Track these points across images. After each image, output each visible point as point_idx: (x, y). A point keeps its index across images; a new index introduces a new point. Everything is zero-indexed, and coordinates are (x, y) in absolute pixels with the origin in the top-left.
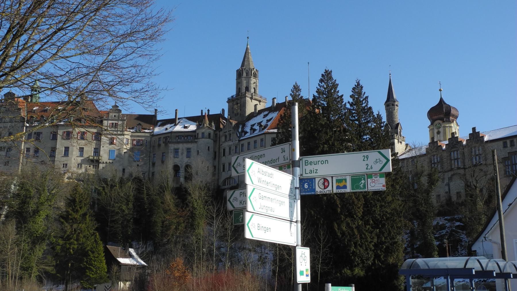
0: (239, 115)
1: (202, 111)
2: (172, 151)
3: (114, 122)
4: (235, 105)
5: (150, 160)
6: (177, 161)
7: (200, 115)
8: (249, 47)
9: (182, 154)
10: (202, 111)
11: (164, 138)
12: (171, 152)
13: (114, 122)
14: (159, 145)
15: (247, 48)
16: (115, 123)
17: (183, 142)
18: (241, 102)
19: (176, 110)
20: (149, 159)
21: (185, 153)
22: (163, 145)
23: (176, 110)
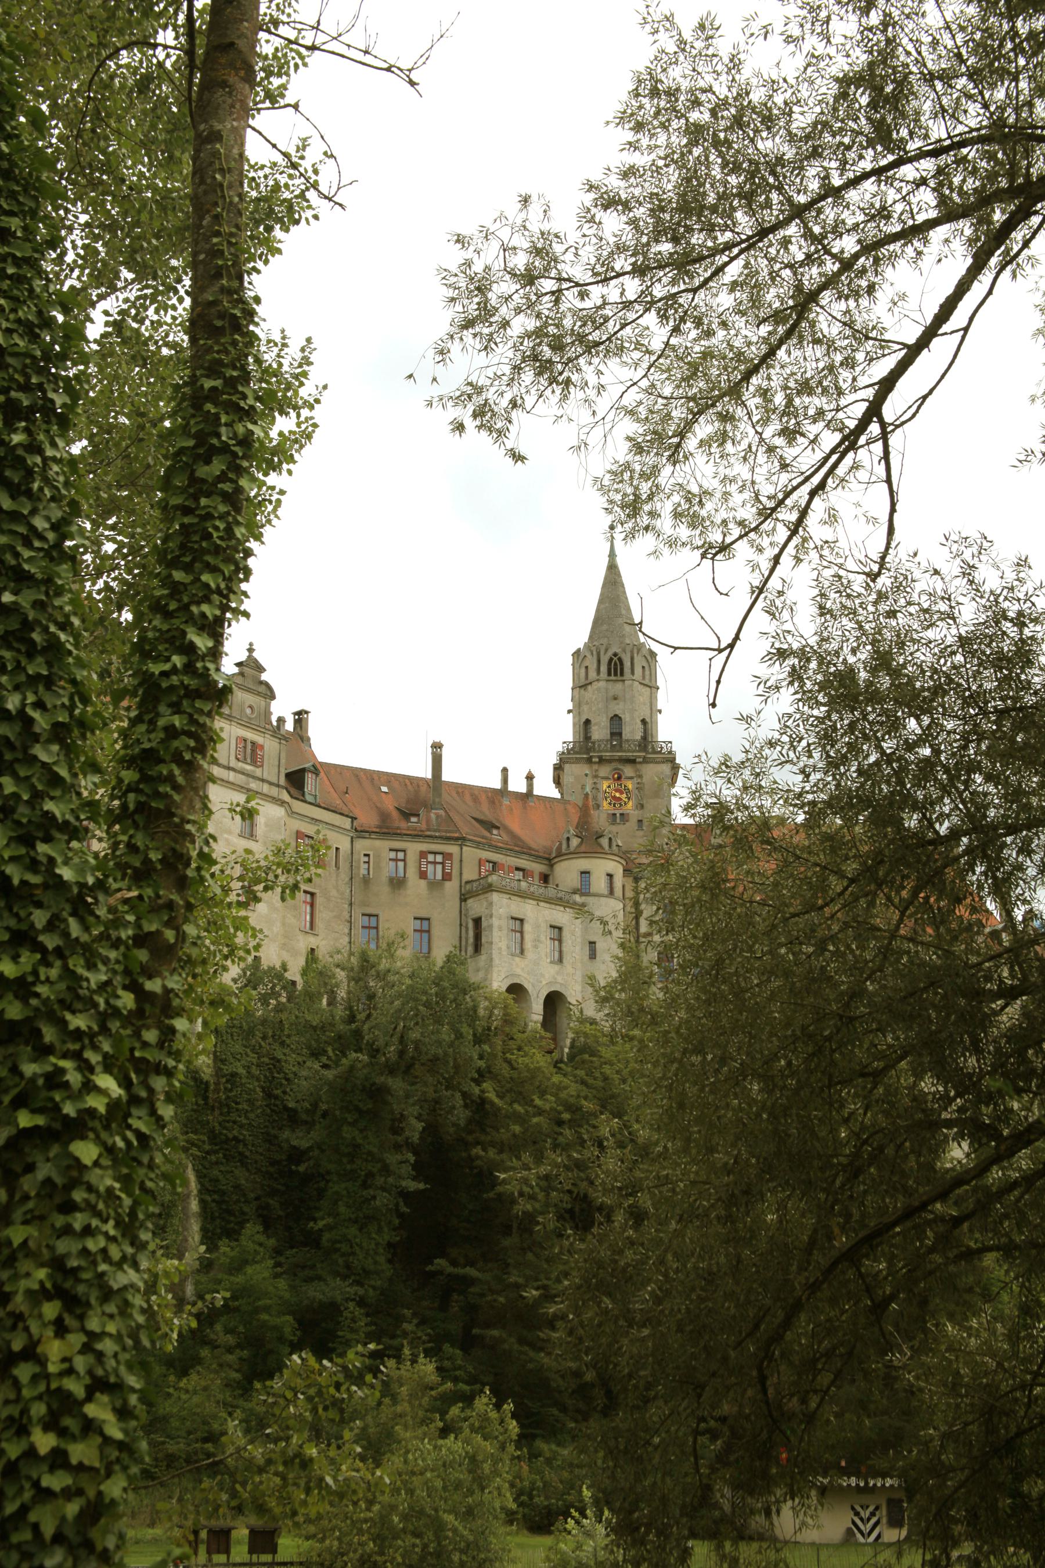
0: (632, 823)
1: (505, 771)
2: (504, 923)
3: (250, 735)
4: (607, 778)
5: (350, 934)
6: (521, 971)
7: (497, 785)
8: (620, 561)
9: (537, 940)
10: (505, 771)
11: (423, 855)
12: (500, 929)
13: (250, 735)
14: (398, 883)
15: (612, 568)
16: (253, 743)
17: (538, 899)
18: (640, 776)
19: (437, 746)
20: (347, 931)
21: (547, 946)
22: (416, 886)
23: (437, 746)
